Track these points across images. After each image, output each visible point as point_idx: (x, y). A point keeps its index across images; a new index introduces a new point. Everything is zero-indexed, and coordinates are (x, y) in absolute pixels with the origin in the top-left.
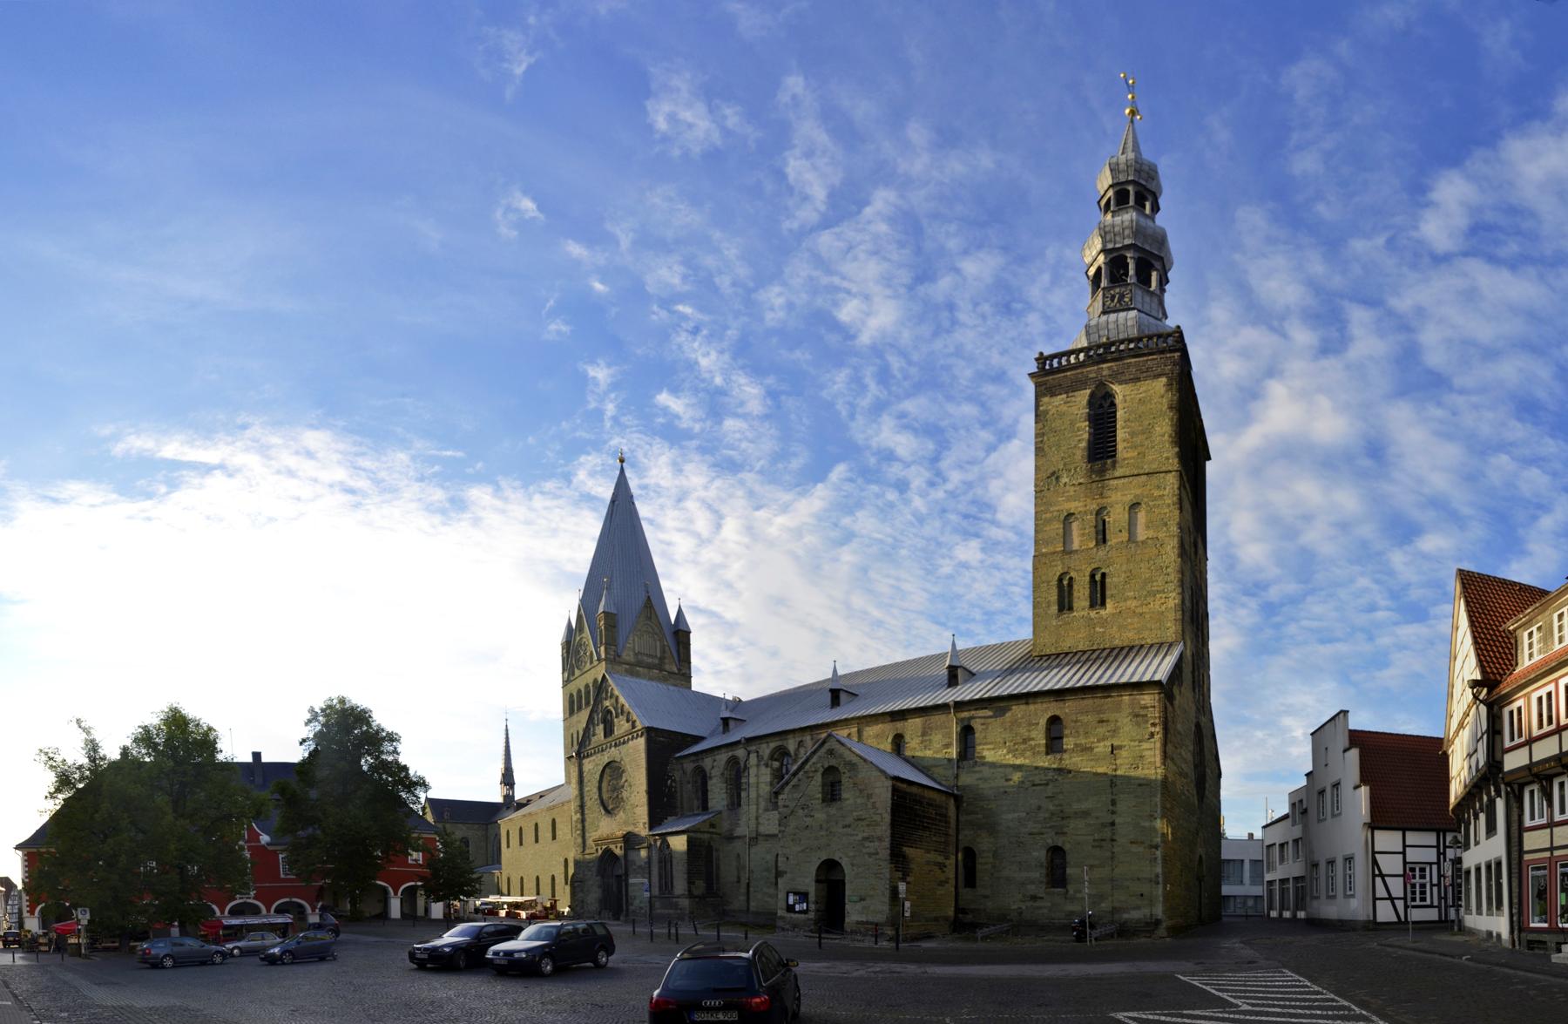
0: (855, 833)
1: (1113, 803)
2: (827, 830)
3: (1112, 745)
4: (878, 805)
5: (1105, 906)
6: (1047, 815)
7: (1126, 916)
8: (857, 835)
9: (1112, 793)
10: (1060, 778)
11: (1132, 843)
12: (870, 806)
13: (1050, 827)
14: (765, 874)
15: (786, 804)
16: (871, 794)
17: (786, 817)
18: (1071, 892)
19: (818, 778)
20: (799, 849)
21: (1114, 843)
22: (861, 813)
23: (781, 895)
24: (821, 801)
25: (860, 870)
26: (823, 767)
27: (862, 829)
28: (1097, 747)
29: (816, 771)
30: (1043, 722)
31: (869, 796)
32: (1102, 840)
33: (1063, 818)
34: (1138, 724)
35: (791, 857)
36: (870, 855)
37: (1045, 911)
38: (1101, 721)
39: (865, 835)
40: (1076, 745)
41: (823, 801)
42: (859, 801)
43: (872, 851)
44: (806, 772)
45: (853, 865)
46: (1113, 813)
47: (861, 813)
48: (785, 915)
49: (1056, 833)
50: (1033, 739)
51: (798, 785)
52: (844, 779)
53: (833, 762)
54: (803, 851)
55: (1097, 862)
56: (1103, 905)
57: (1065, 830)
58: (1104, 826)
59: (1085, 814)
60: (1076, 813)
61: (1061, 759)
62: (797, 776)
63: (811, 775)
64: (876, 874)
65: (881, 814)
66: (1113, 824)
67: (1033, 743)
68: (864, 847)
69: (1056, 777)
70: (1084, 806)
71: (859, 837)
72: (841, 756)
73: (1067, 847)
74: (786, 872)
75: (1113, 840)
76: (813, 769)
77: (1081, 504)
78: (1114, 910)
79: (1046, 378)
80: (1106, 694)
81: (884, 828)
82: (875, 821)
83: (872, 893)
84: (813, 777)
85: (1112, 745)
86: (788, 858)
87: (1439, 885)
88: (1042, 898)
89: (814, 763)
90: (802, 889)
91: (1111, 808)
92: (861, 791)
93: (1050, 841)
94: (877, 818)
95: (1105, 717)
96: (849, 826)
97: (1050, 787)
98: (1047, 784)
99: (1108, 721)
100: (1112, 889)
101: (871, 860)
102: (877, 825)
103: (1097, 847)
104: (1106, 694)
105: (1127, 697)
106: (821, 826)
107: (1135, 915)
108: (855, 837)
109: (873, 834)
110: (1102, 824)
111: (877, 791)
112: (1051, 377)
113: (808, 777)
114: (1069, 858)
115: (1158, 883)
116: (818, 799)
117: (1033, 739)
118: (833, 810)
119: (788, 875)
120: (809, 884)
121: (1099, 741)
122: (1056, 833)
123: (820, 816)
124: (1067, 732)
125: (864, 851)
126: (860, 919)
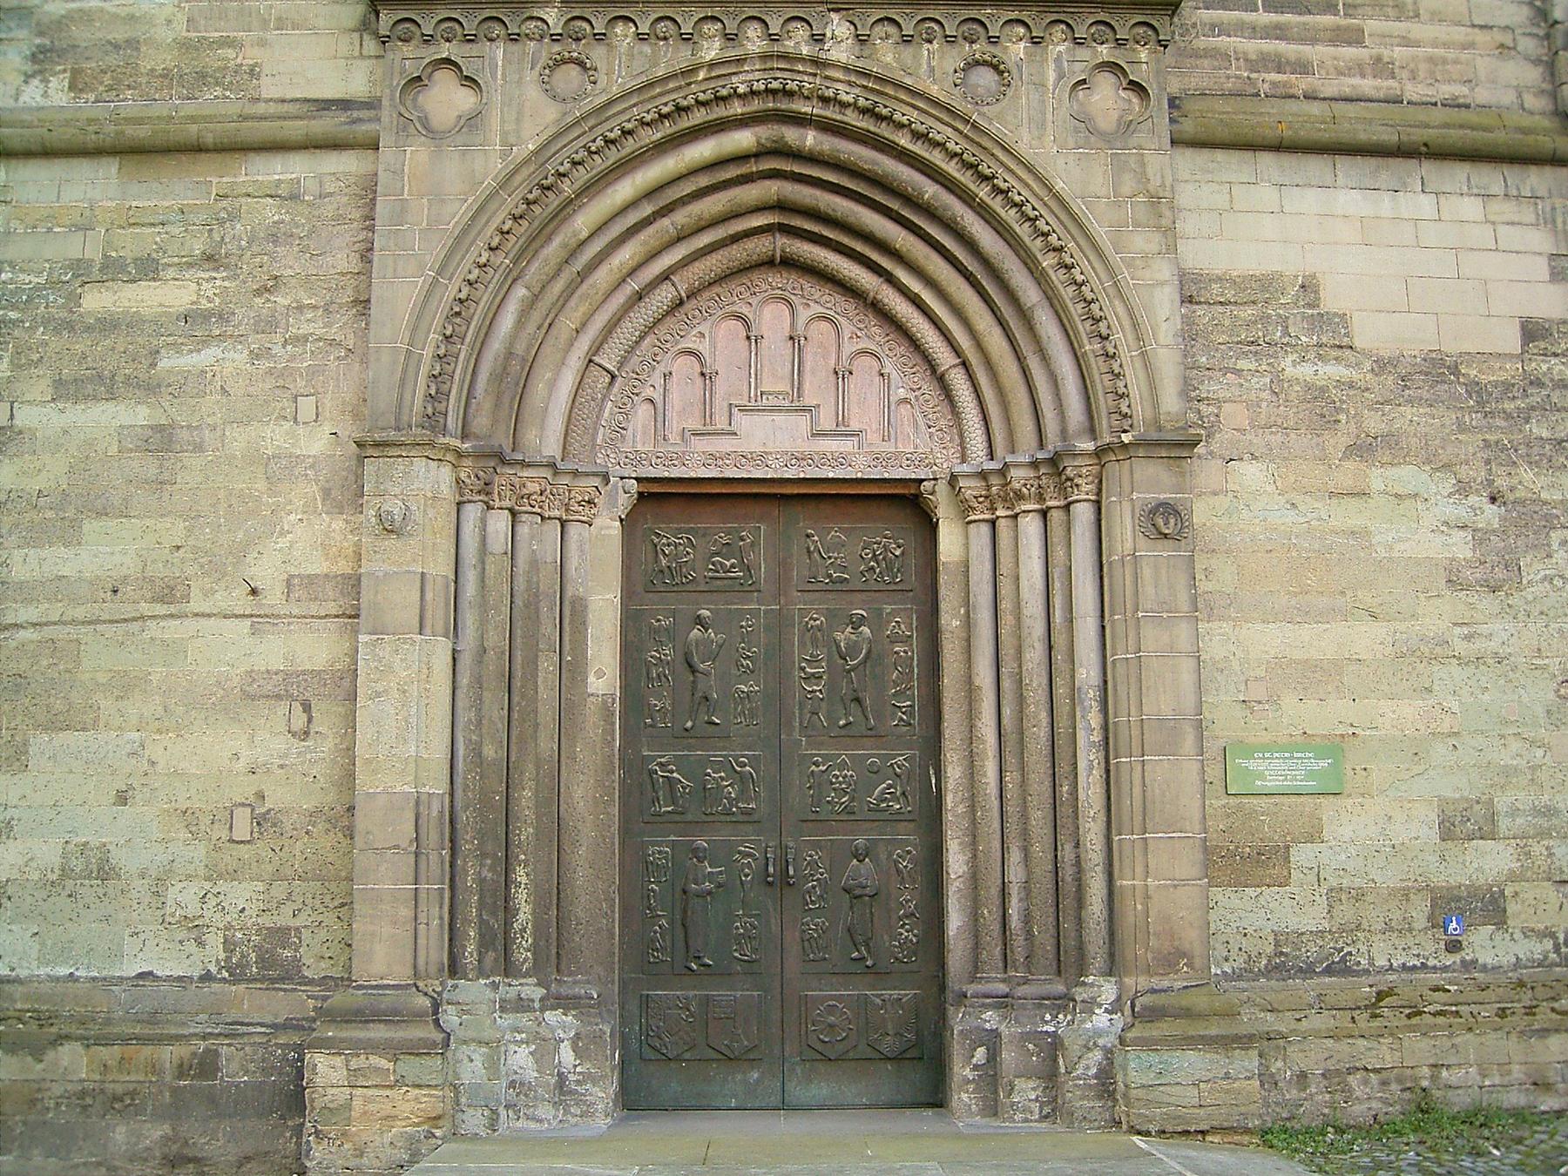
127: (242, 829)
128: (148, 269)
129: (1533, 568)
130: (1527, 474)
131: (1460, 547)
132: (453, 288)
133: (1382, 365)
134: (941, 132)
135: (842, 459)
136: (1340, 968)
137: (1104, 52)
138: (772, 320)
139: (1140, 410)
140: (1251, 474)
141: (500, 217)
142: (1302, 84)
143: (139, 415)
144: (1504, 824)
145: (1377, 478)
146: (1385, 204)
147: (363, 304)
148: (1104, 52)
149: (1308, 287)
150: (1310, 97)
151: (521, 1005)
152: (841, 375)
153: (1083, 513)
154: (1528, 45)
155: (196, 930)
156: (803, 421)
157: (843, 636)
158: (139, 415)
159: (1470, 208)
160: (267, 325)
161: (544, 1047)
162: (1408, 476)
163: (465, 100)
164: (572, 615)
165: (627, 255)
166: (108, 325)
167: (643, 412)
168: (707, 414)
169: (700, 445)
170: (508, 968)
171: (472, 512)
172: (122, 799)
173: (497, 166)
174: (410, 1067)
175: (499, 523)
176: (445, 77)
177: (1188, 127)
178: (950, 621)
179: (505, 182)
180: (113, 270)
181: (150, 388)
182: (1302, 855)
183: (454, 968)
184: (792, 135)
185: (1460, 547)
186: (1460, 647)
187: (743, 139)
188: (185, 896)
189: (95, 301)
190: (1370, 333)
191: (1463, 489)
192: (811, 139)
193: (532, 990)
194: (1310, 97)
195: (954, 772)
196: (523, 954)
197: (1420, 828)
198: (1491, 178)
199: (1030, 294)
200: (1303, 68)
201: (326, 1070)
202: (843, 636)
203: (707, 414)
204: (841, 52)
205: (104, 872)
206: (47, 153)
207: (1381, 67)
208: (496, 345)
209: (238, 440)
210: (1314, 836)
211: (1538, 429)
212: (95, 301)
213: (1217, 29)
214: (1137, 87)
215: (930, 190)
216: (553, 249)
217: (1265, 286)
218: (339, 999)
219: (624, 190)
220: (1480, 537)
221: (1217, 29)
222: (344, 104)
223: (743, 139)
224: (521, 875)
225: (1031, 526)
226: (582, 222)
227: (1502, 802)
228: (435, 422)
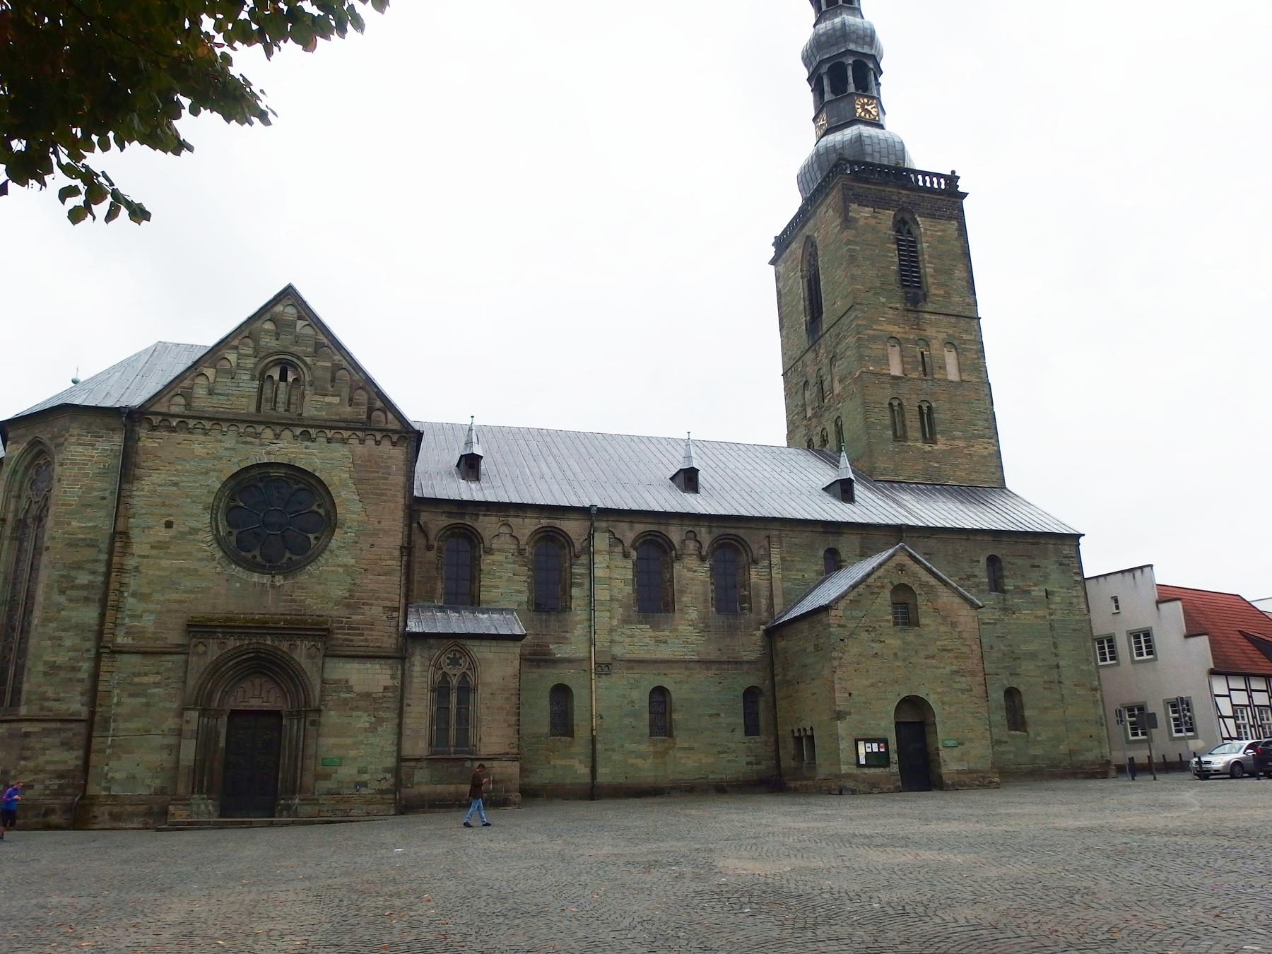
0: (942, 665)
1: (1055, 647)
2: (904, 661)
3: (1046, 591)
4: (965, 635)
5: (1063, 748)
6: (1000, 655)
7: (1082, 758)
8: (944, 668)
9: (1053, 637)
10: (1006, 618)
11: (1076, 685)
12: (956, 635)
13: (1005, 667)
14: (627, 721)
15: (842, 622)
16: (955, 622)
17: (843, 640)
18: (1032, 735)
19: (886, 595)
20: (868, 683)
21: (1062, 685)
22: (946, 643)
23: (845, 745)
24: (892, 624)
25: (953, 709)
26: (891, 583)
27: (949, 661)
28: (1034, 591)
29: (883, 587)
30: (983, 560)
31: (954, 625)
32: (1050, 682)
33: (1014, 659)
34: (1063, 572)
35: (855, 693)
36: (963, 691)
37: (1011, 756)
38: (1033, 566)
39: (954, 668)
40: (1017, 587)
41: (896, 624)
42: (942, 629)
43: (964, 686)
44: (868, 586)
45: (943, 703)
46: (1056, 656)
47: (946, 643)
48: (855, 772)
49: (1011, 674)
50: (976, 576)
51: (858, 601)
52: (921, 601)
53: (905, 580)
54: (872, 685)
55: (1050, 705)
56: (1061, 747)
57: (1018, 671)
58: (1050, 667)
59: (1033, 656)
60: (1024, 654)
61: (1005, 600)
62: (856, 590)
63: (876, 590)
64: (973, 713)
65: (970, 646)
66: (1058, 666)
67: (977, 580)
68: (954, 682)
69: (1002, 617)
70: (1032, 647)
71: (948, 669)
72: (915, 575)
73: (1022, 688)
74: (850, 714)
75: (1060, 682)
76: (879, 584)
77: (900, 330)
78: (1071, 753)
79: (853, 184)
80: (1035, 541)
81: (975, 661)
82: (962, 653)
83: (970, 735)
84: (879, 594)
85: (1046, 591)
86: (850, 694)
87: (1254, 726)
88: (1006, 742)
89: (879, 577)
90: (879, 734)
91: (1054, 650)
92: (944, 618)
93: (1005, 682)
94: (965, 649)
95: (1036, 562)
96: (933, 657)
97: (998, 626)
98: (995, 624)
99: (1038, 567)
100: (1067, 731)
101: (964, 697)
102: (968, 657)
103: (1047, 689)
104: (1035, 541)
105: (1051, 546)
106: (895, 654)
107: (1090, 756)
108: (942, 670)
109: (963, 667)
110: (1049, 666)
111: (962, 619)
112: (857, 184)
113: (873, 593)
114: (1025, 699)
115: (1102, 725)
116: (888, 621)
117: (976, 576)
118: (910, 636)
119: (853, 716)
120: (886, 725)
121: (1035, 585)
122: (1011, 674)
123: (894, 642)
124: (1006, 573)
125: (955, 686)
126: (960, 768)
127: (159, 770)
128: (146, 674)
129: (379, 729)
130: (381, 713)
131: (367, 725)
132: (200, 682)
133: (358, 694)
134: (285, 656)
135: (266, 707)
136: (339, 794)
137: (312, 643)
138: (257, 682)
139: (312, 704)
140: (332, 713)
141: (208, 670)
142: (351, 644)
143: (144, 700)
144: (369, 771)
145: (354, 713)
146: (362, 666)
147: (185, 682)
148: (312, 643)
149: (347, 681)
150: (353, 646)
151: (203, 799)
152: (268, 692)
153: (303, 720)
154: (395, 636)
155: (149, 786)
156: (261, 700)
157: (265, 737)
158: (144, 700)
159: (378, 667)
160: (167, 685)
161: (207, 806)
162: (360, 713)
163: (204, 648)
164: (218, 734)
165: (231, 672)
166: (138, 684)
167: (233, 698)
168: (244, 698)
169: (243, 704)
170: (202, 793)
171: (201, 718)
172: (138, 765)
173: (209, 662)
174: (186, 807)
175: (206, 720)
176: (201, 645)
177: (329, 653)
178: (283, 735)
179: (210, 664)
180: (139, 674)
181: (146, 696)
182: (334, 775)
183: (193, 793)
184: (260, 655)
185: (367, 725)
186: (365, 742)
187: (252, 655)
188: (148, 781)
189: (136, 680)
190: (356, 689)
191: (369, 715)
192: (263, 655)
193: (205, 796)
194: (353, 646)
195: (281, 761)
196: (205, 791)
197: (354, 771)
198: (383, 662)
199: (298, 683)
200: (352, 641)
201: (171, 808)
202: (265, 737)
203: (244, 698)
204: (269, 642)
205: (134, 777)
206: (129, 653)
207: (366, 640)
208: (207, 690)
209: (161, 705)
210: (336, 773)
211: (384, 705)
212: (136, 680)
213: (338, 634)
214: (318, 649)
215: (283, 664)
216: (218, 673)
217: (340, 681)
218: (174, 797)
219: (231, 663)
220: (371, 724)
221: (338, 634)
222: (183, 645)
223: (252, 655)
224: (205, 778)
225: (296, 721)
226: (223, 669)
227: (369, 767)
228: (196, 704)
